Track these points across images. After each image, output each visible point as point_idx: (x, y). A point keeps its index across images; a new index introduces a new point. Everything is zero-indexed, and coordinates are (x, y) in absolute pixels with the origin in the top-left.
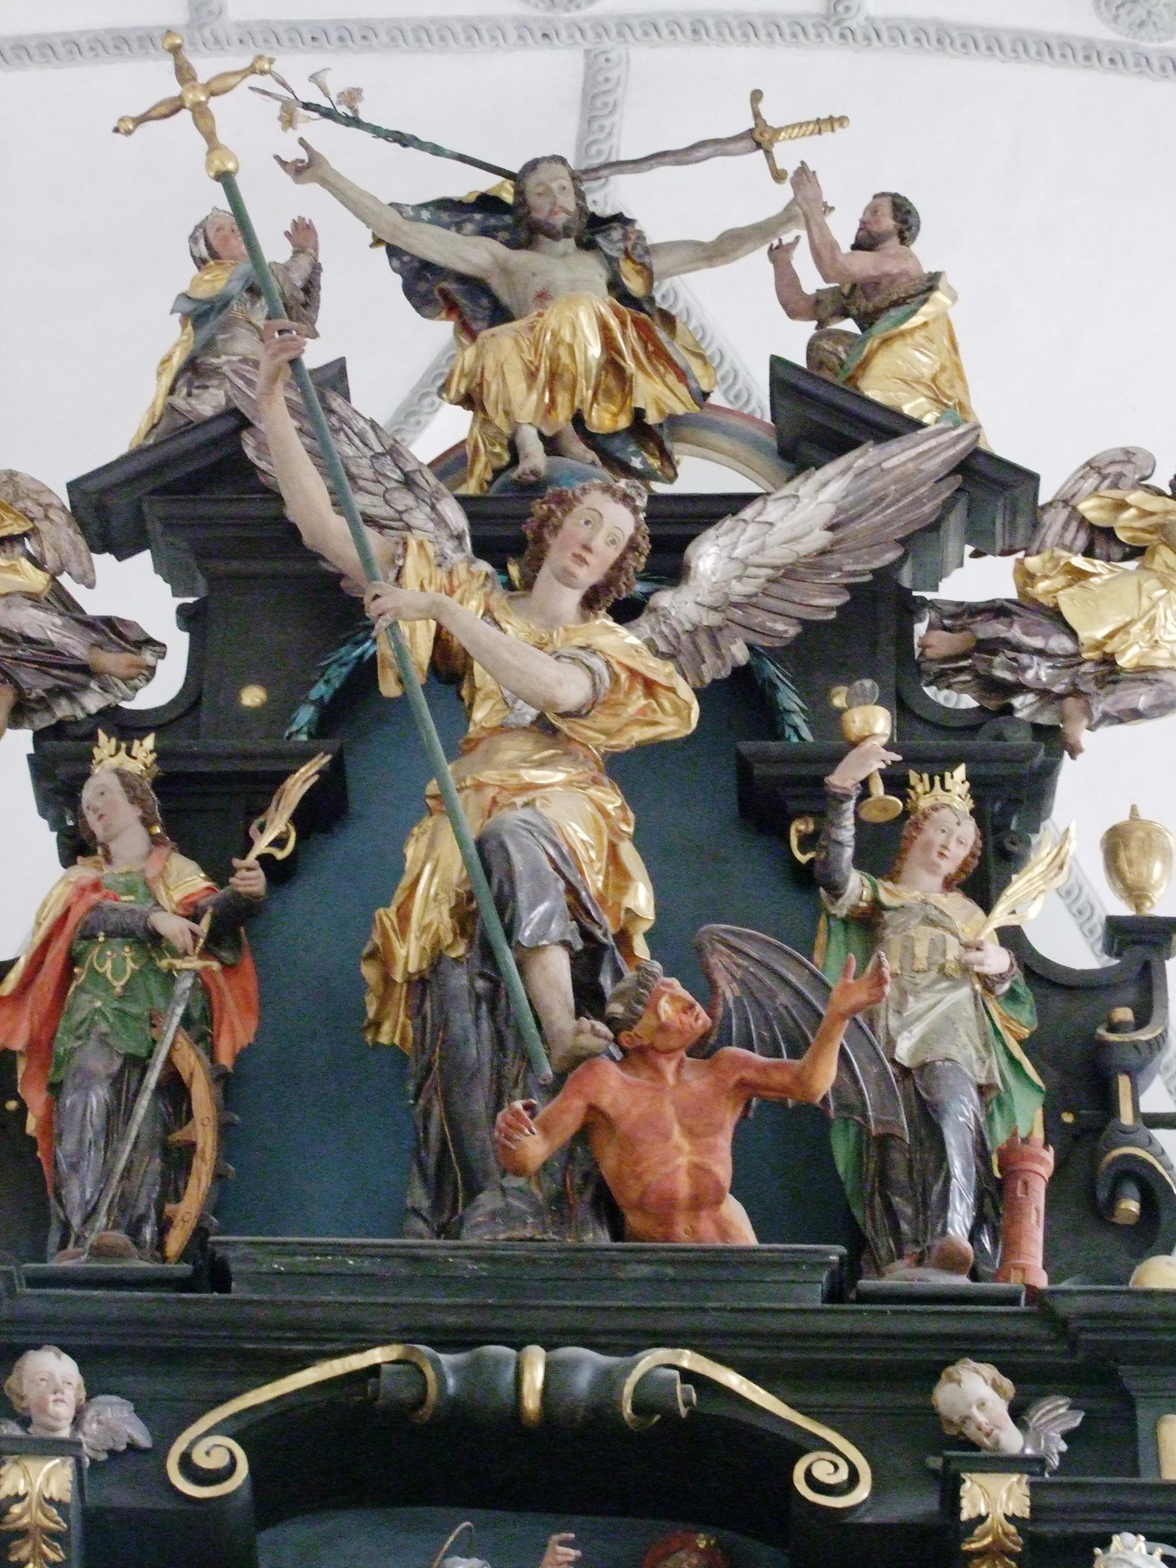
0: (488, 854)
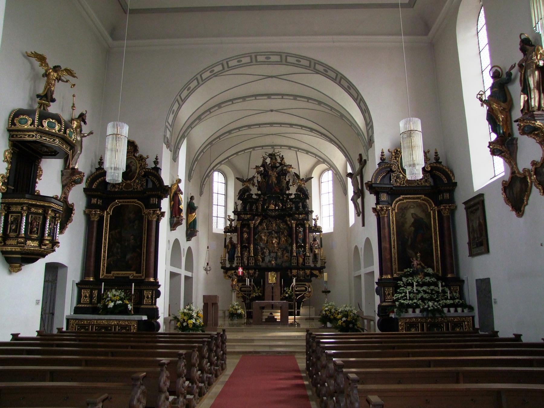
0: (272, 182)
